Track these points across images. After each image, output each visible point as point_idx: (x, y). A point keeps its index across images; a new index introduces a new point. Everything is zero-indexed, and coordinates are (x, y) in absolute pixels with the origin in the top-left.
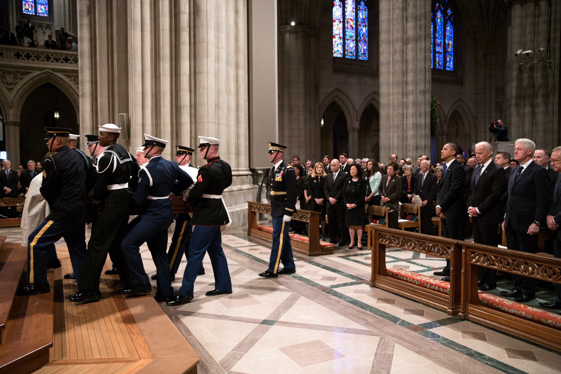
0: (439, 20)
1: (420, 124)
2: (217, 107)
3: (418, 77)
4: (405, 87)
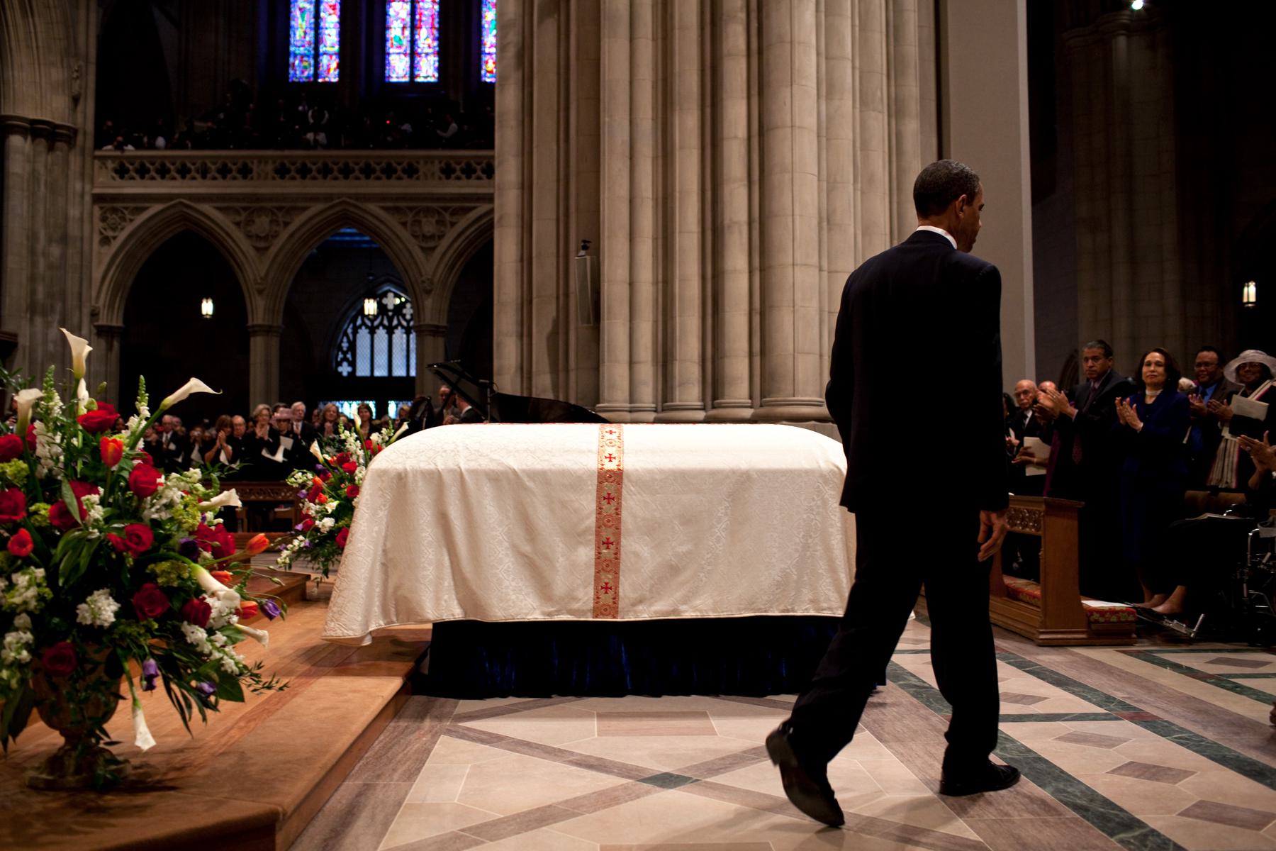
2: (825, 224)
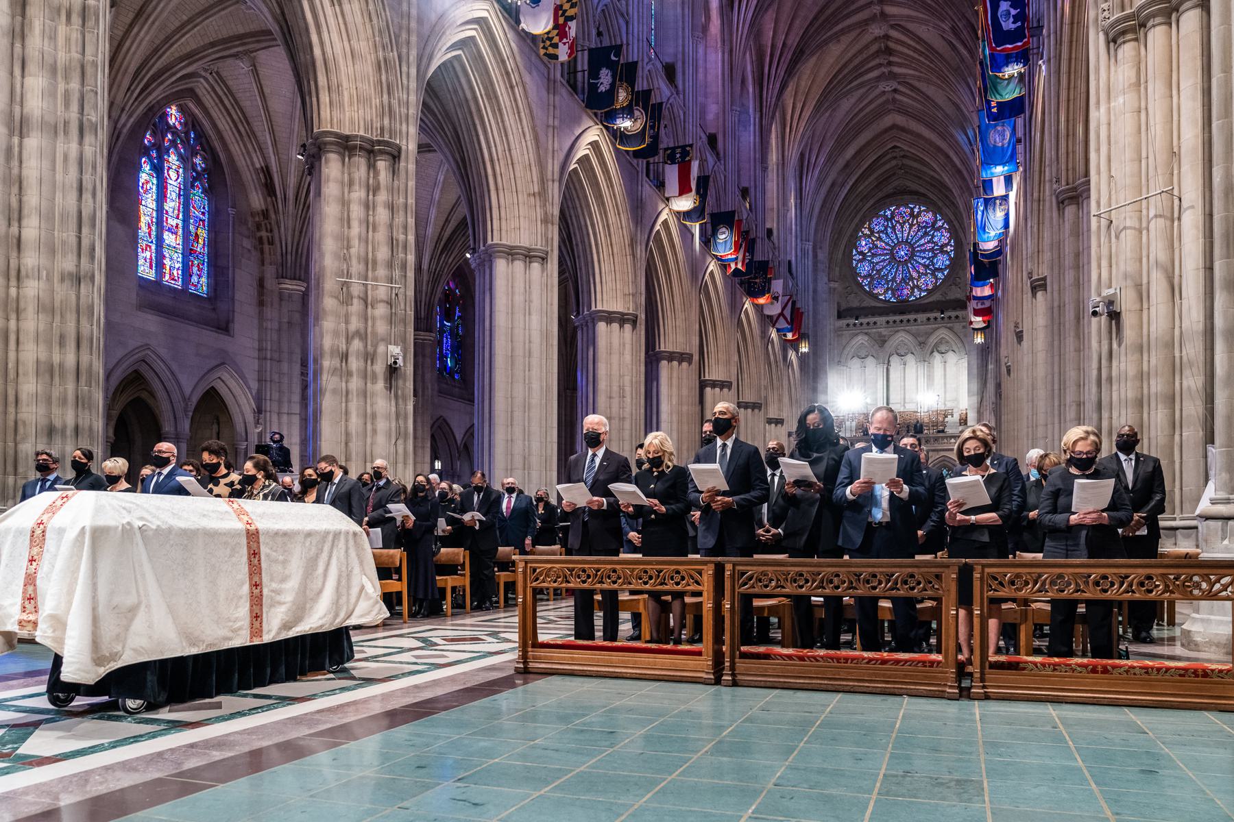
0: (173, 175)
1: (61, 365)
3: (56, 233)
4: (14, 254)
